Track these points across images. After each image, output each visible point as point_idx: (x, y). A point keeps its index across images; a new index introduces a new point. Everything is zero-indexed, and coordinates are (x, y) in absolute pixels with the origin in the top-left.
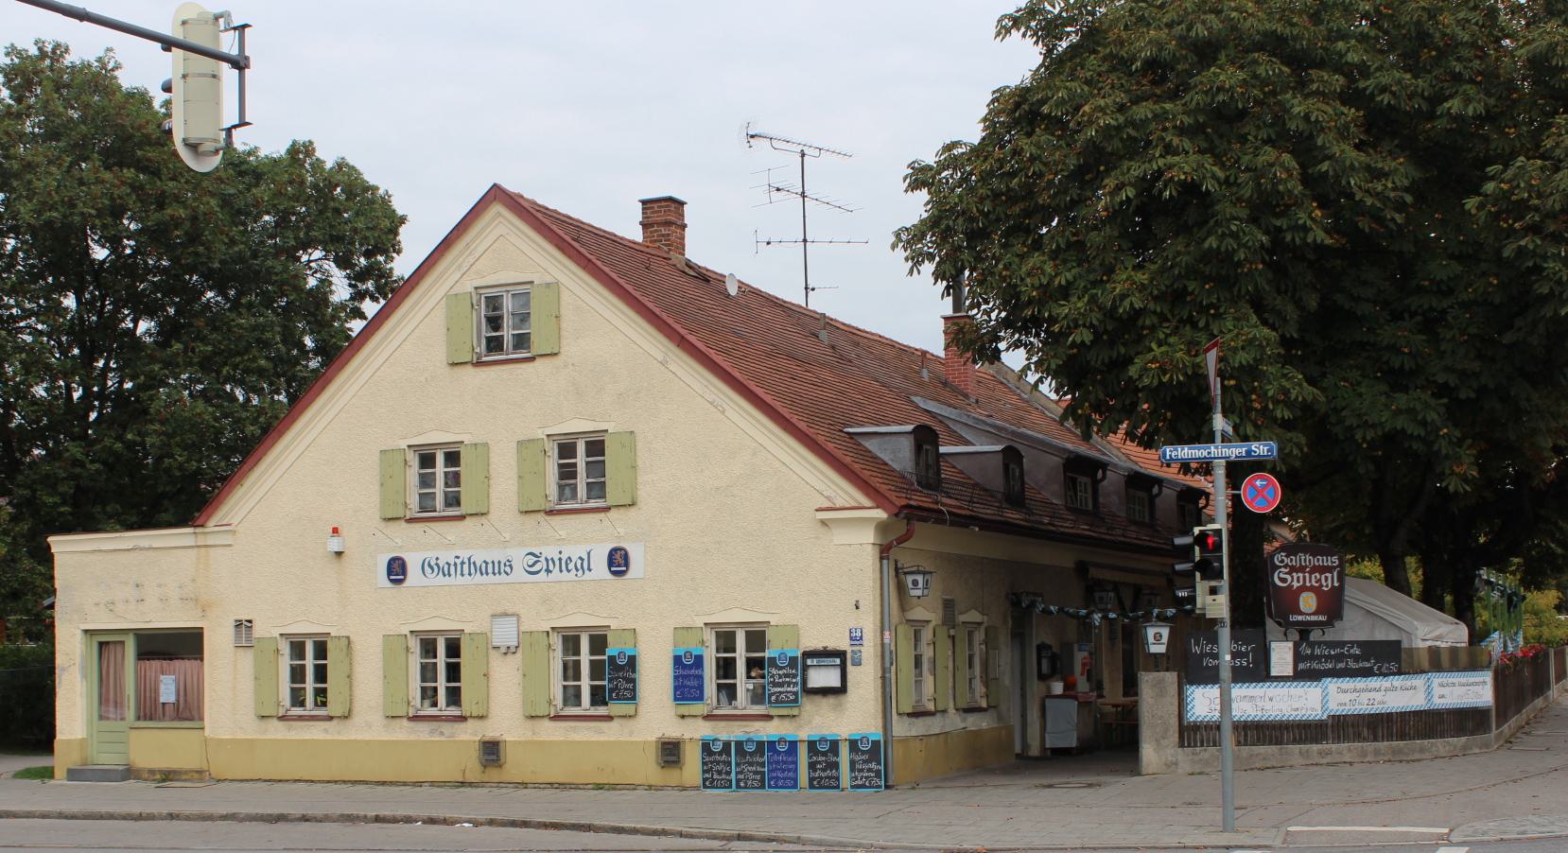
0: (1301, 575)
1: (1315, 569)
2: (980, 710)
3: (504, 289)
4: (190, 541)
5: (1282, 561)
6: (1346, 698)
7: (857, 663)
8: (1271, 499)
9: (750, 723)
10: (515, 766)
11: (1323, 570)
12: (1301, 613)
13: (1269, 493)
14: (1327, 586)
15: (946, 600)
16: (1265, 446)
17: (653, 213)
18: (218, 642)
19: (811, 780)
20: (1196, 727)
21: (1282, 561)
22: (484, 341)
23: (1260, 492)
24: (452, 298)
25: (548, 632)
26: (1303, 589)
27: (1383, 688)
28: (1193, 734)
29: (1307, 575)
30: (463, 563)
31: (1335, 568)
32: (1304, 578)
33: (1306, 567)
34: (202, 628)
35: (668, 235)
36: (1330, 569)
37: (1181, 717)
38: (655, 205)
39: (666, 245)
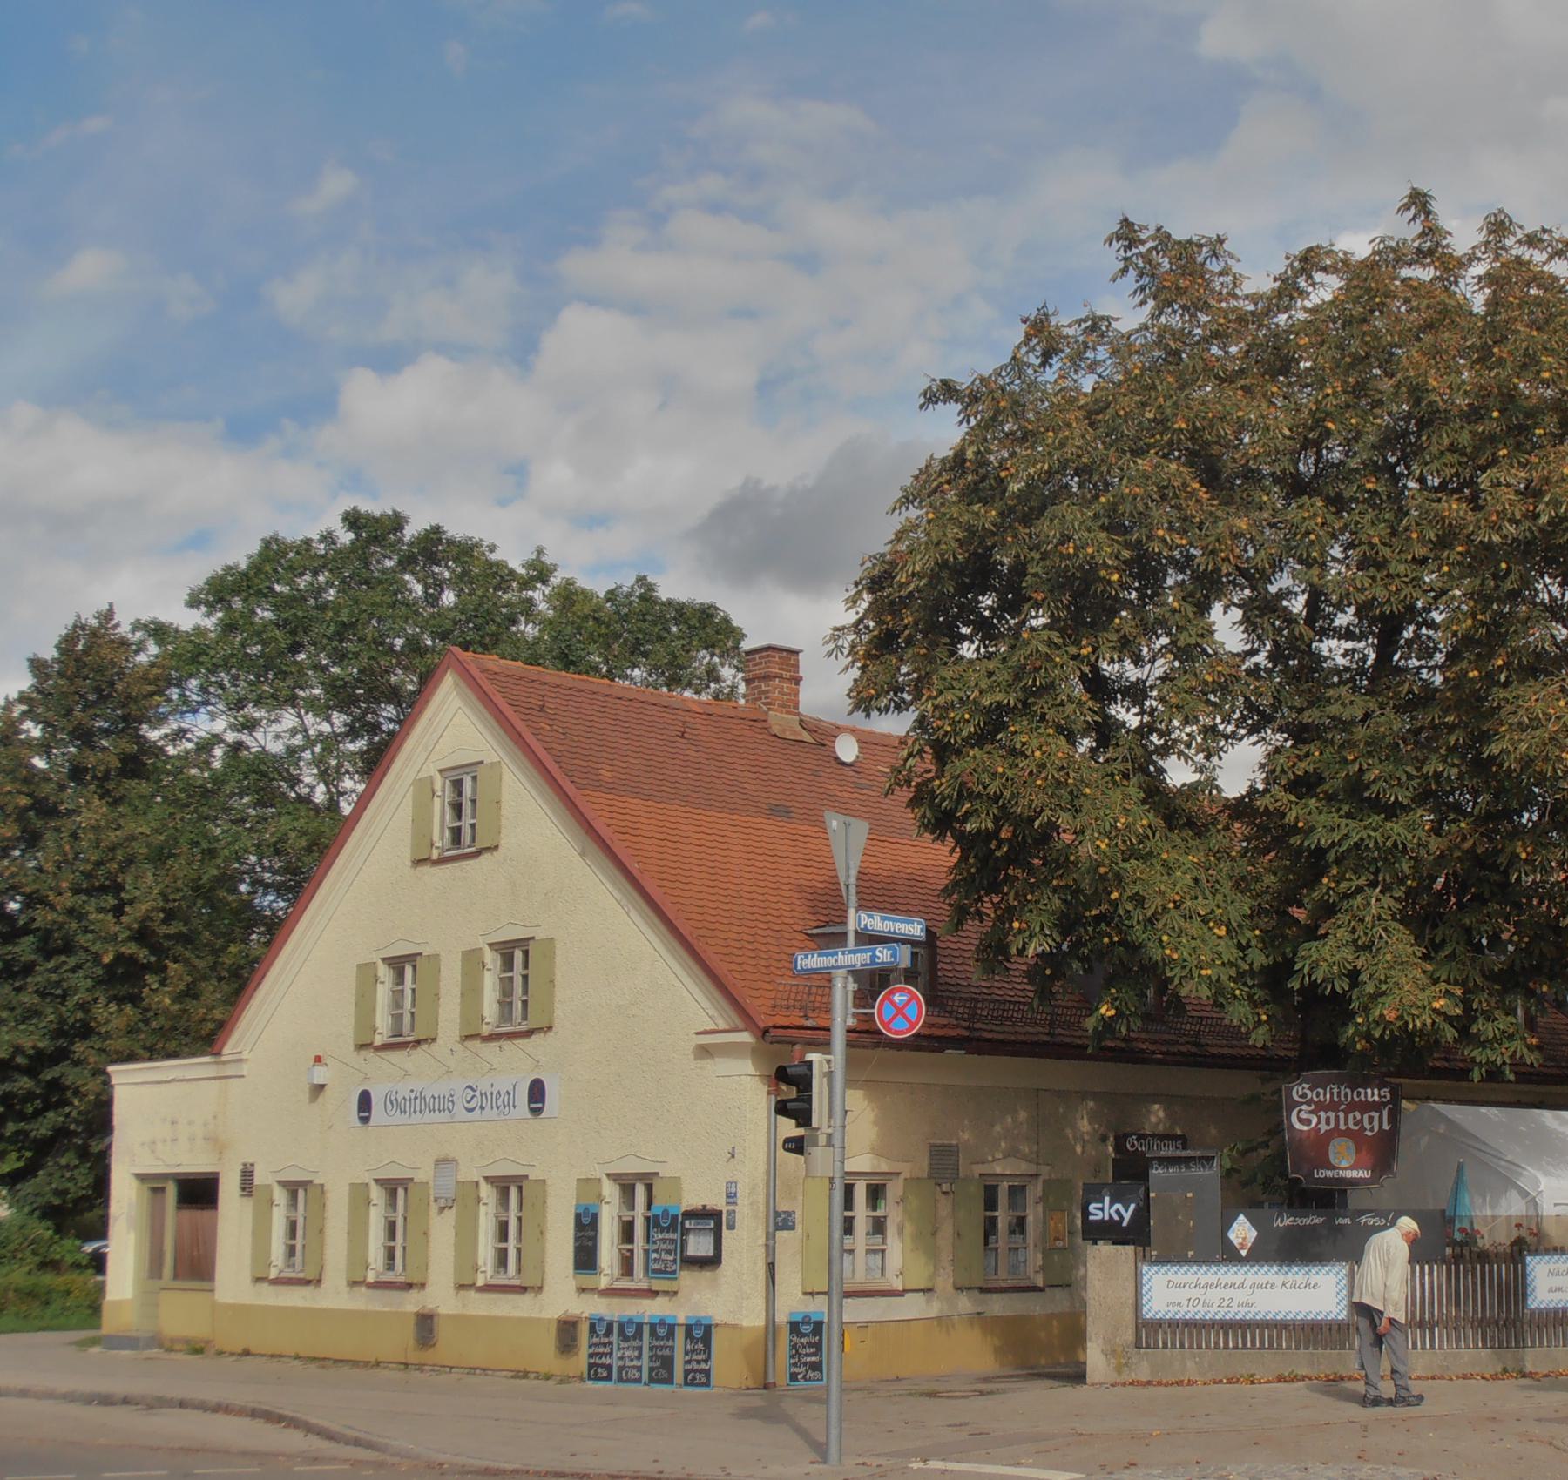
0: (1332, 1114)
1: (1352, 1107)
2: (1035, 1289)
3: (461, 771)
4: (211, 1071)
5: (1304, 1096)
6: (1182, 1295)
7: (731, 1227)
8: (913, 1020)
9: (638, 1301)
10: (448, 1343)
11: (1366, 1107)
12: (1334, 1168)
13: (912, 1011)
14: (1372, 1130)
15: (932, 1146)
16: (889, 949)
17: (755, 665)
18: (229, 1190)
19: (687, 1372)
20: (1156, 1325)
21: (1304, 1096)
22: (447, 833)
23: (900, 1011)
24: (424, 788)
25: (477, 1183)
26: (1335, 1132)
27: (1248, 1284)
28: (1150, 1332)
29: (1341, 1115)
30: (416, 1098)
31: (1384, 1104)
32: (1337, 1118)
33: (1340, 1103)
34: (217, 1173)
35: (767, 691)
36: (1377, 1107)
37: (1138, 1306)
38: (757, 656)
39: (764, 704)
